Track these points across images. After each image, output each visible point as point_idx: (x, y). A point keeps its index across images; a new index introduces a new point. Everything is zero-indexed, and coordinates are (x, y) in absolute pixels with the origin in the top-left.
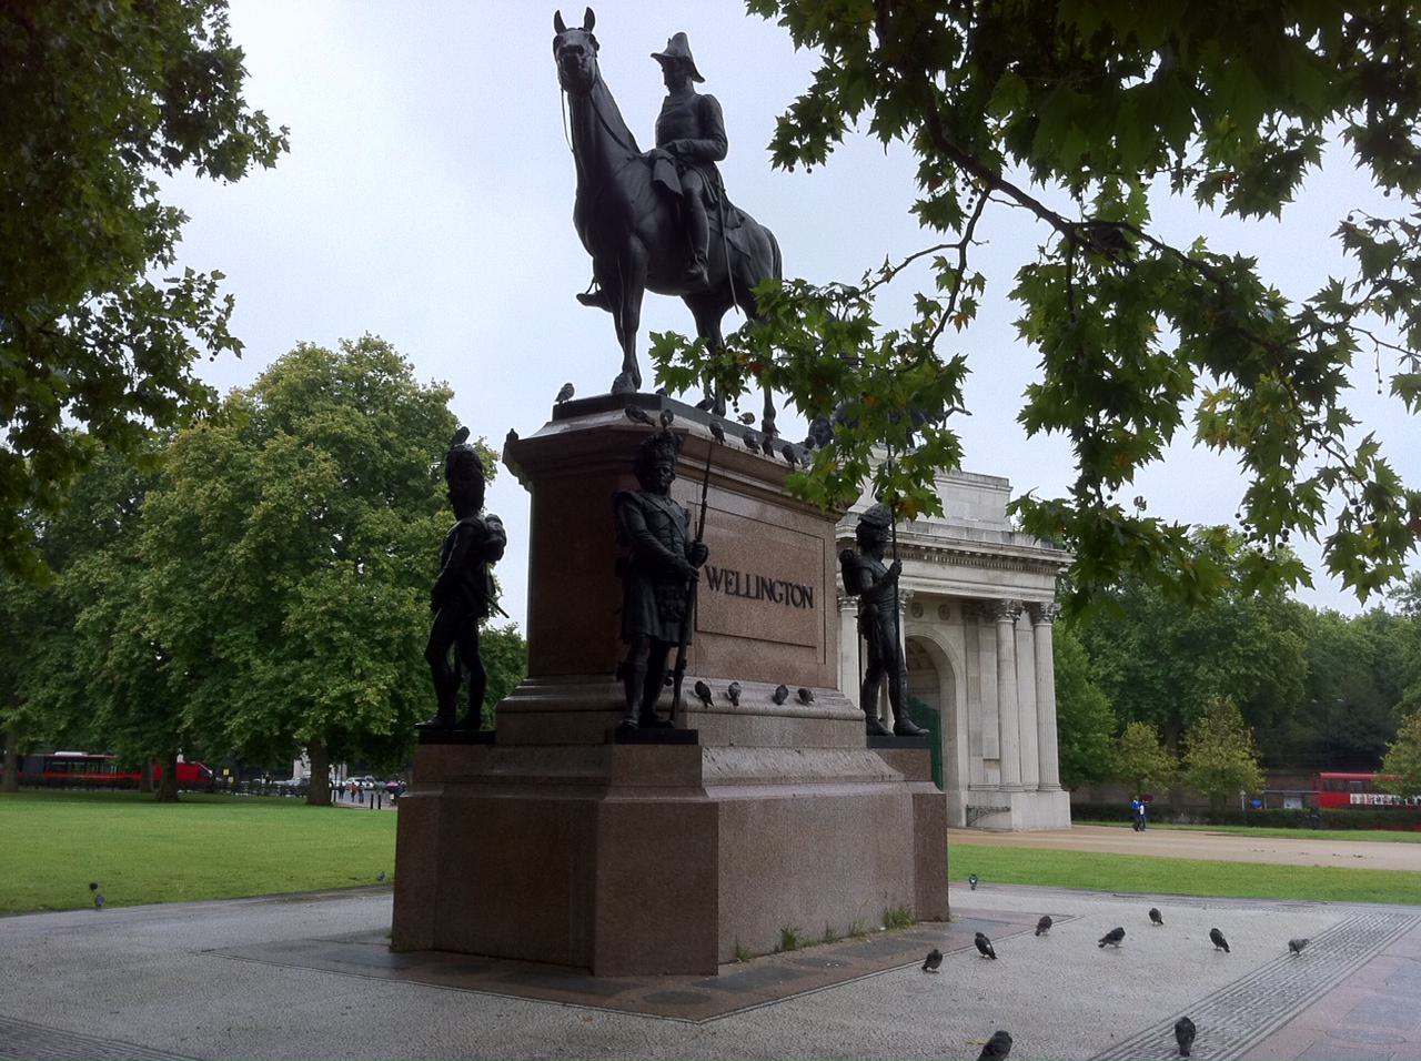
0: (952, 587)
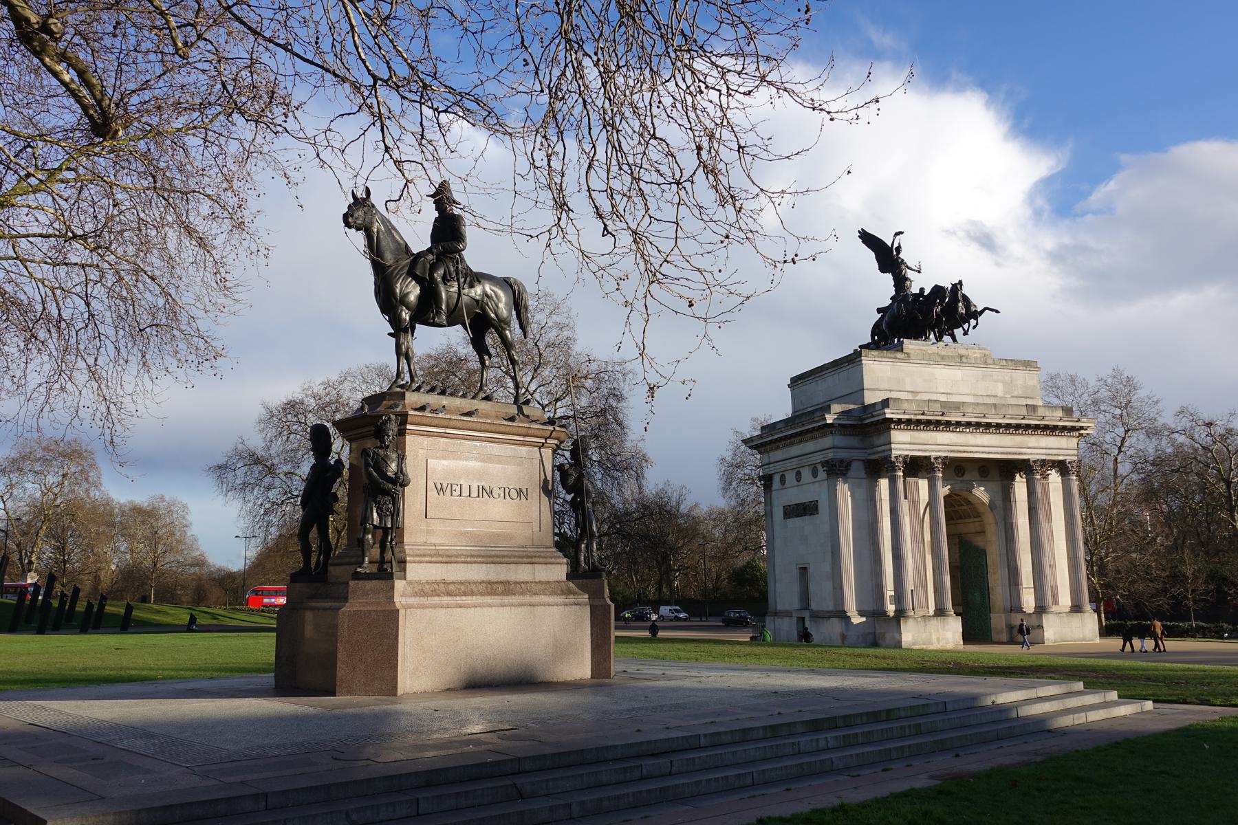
0: (983, 452)
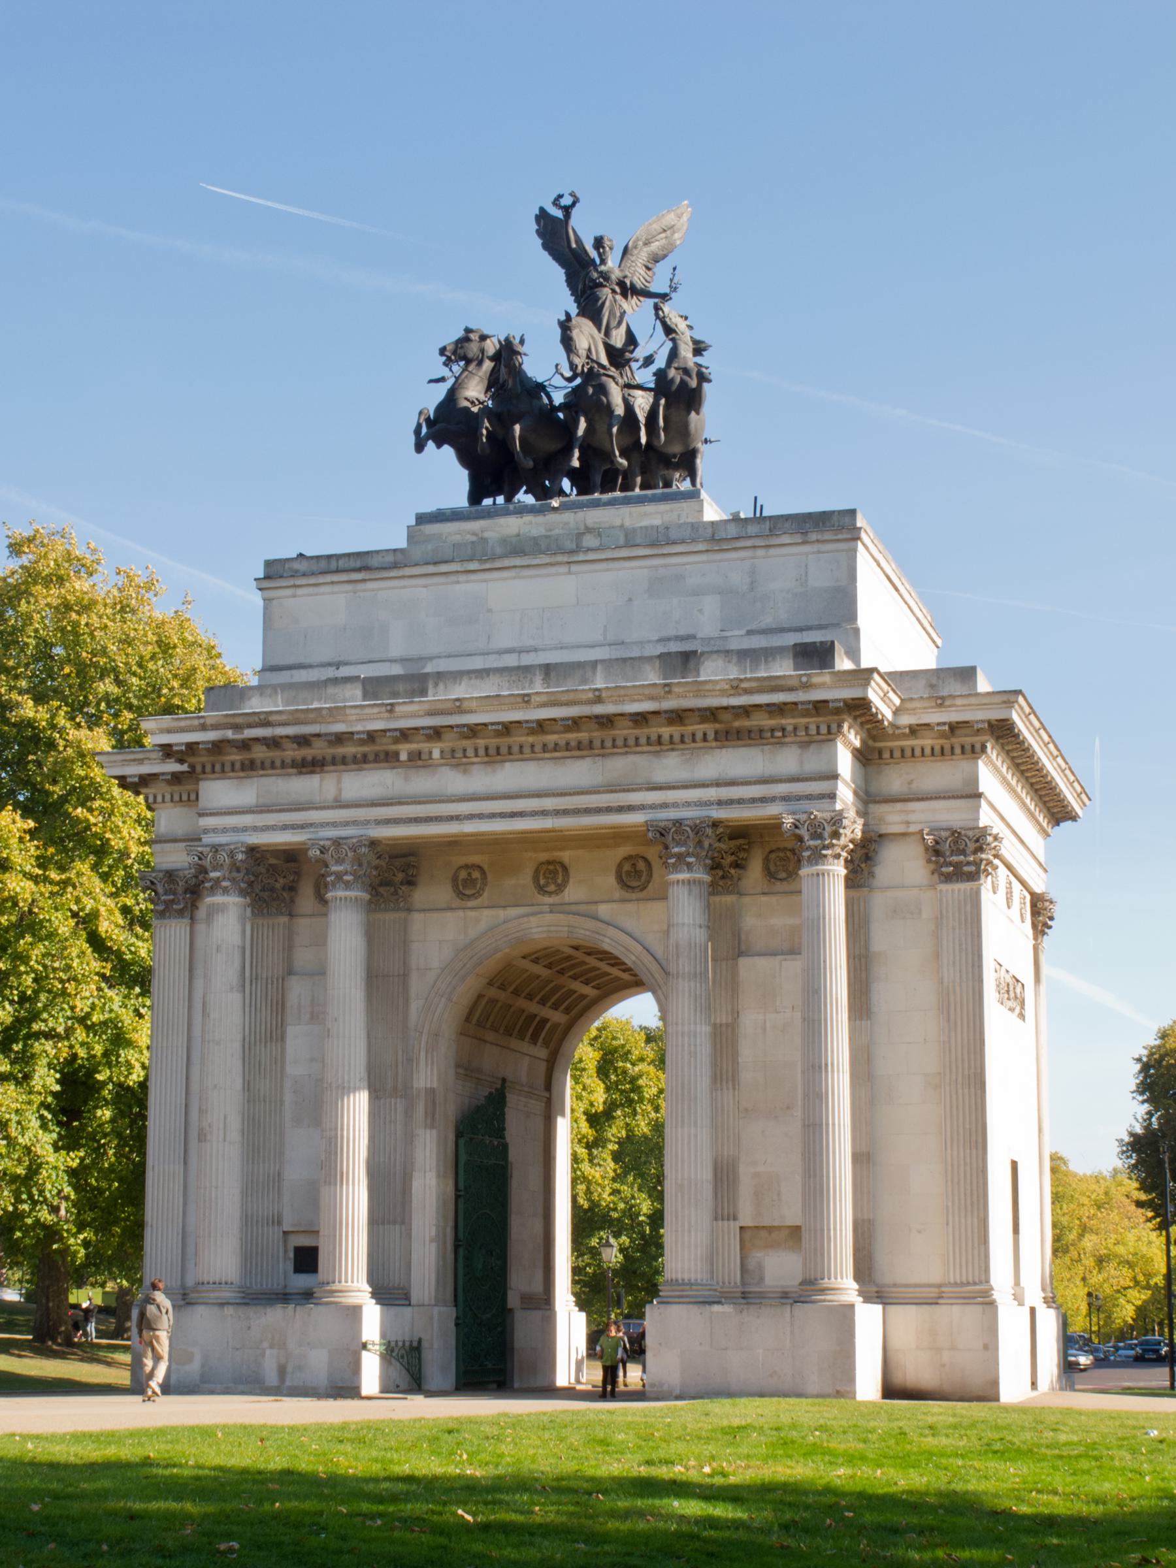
0: (492, 816)
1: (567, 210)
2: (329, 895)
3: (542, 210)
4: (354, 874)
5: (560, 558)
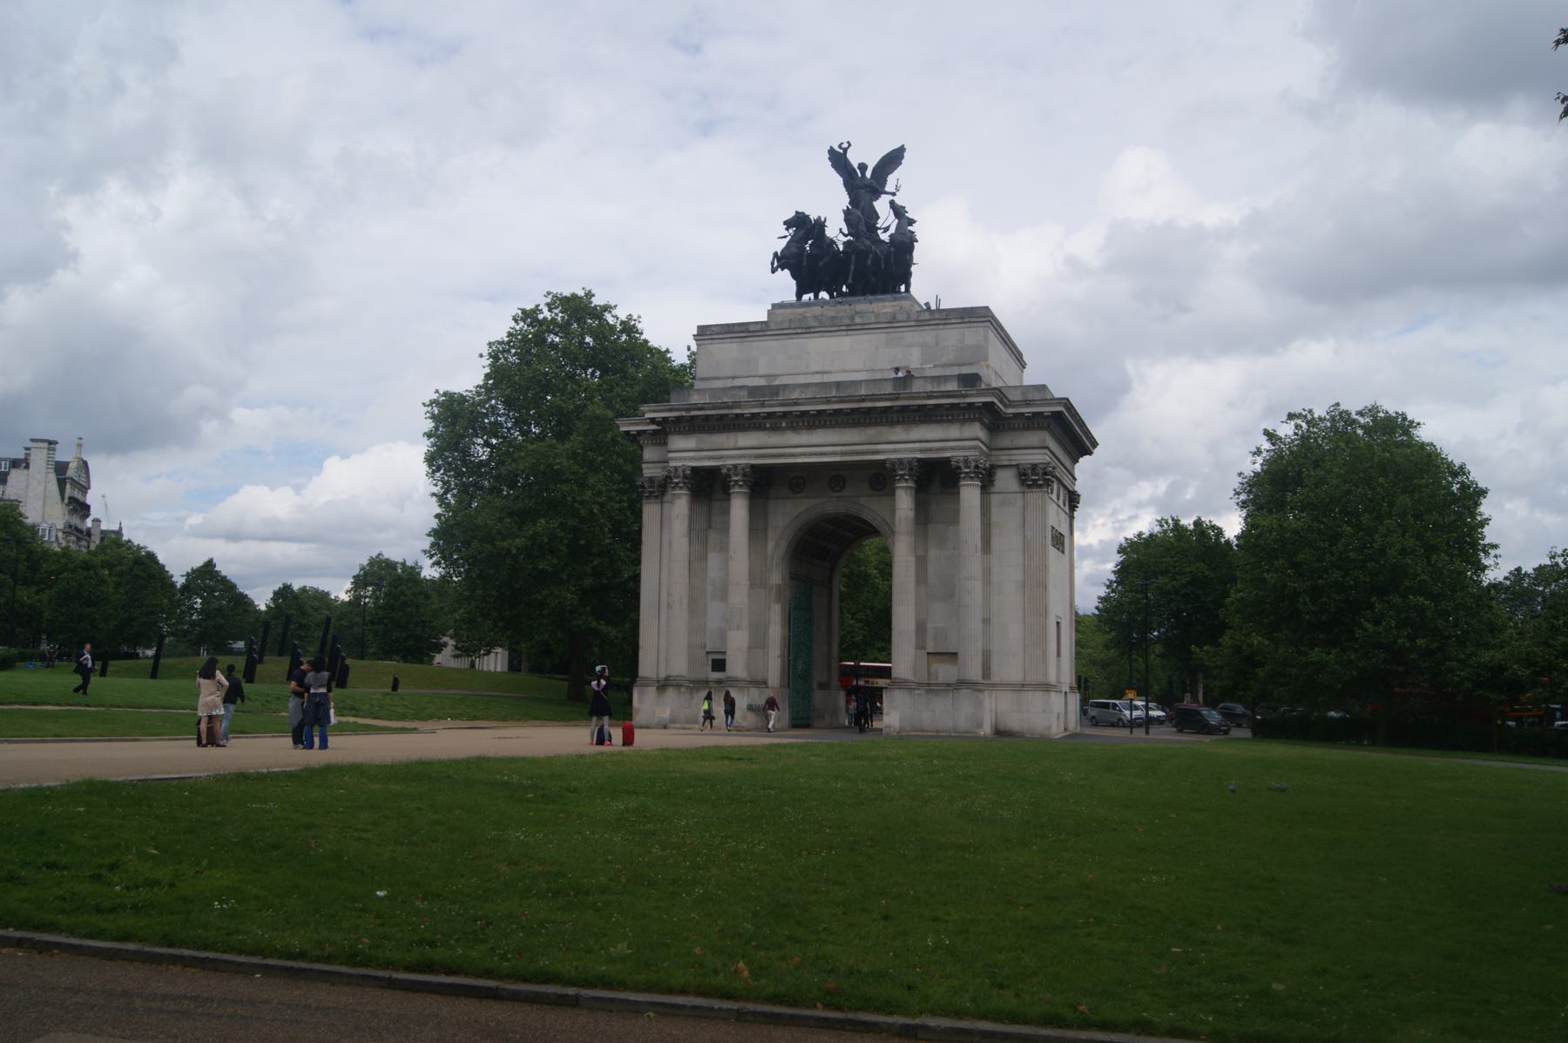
0: (811, 454)
1: (845, 150)
2: (732, 491)
3: (831, 147)
4: (743, 481)
5: (842, 328)
